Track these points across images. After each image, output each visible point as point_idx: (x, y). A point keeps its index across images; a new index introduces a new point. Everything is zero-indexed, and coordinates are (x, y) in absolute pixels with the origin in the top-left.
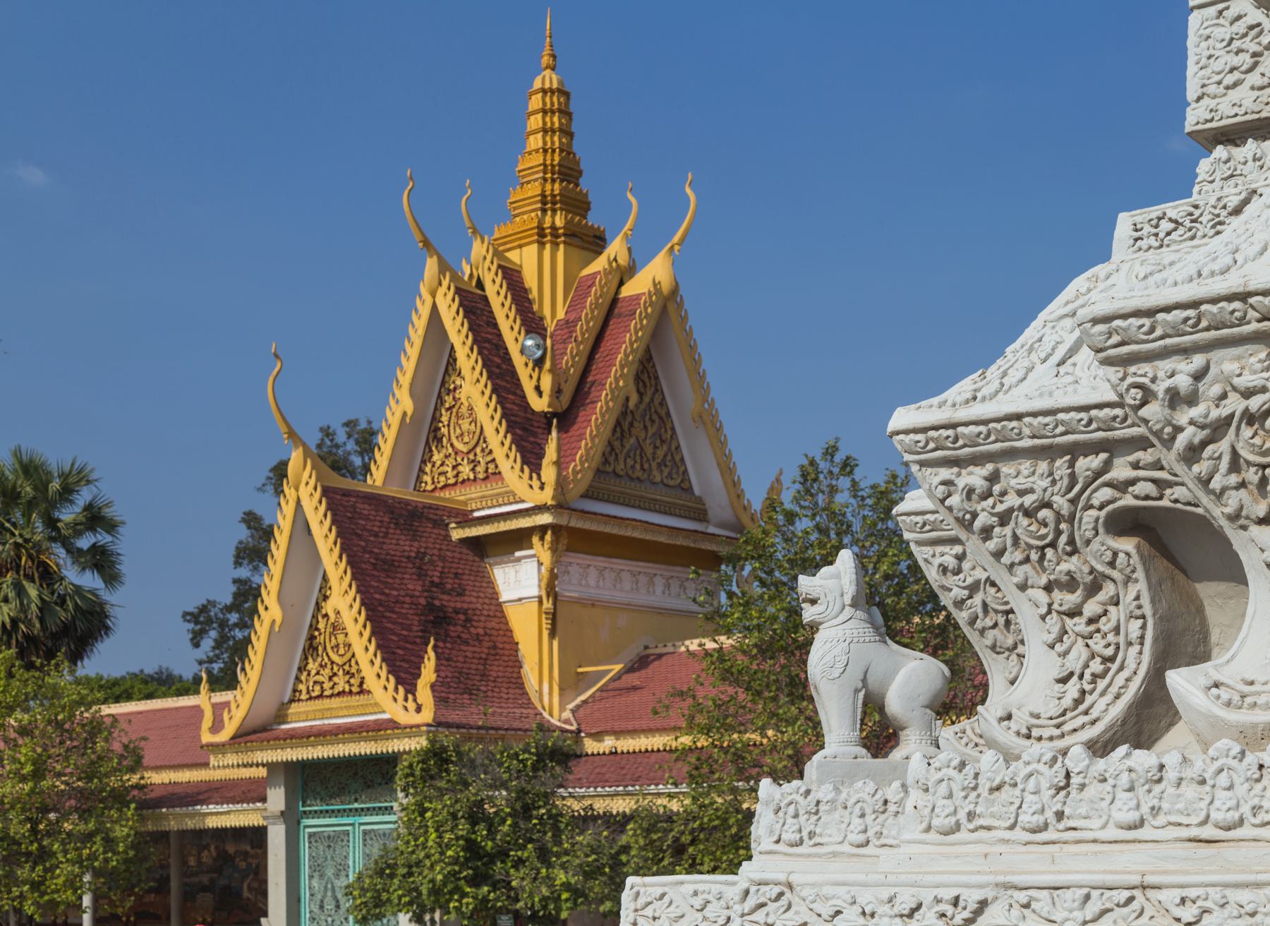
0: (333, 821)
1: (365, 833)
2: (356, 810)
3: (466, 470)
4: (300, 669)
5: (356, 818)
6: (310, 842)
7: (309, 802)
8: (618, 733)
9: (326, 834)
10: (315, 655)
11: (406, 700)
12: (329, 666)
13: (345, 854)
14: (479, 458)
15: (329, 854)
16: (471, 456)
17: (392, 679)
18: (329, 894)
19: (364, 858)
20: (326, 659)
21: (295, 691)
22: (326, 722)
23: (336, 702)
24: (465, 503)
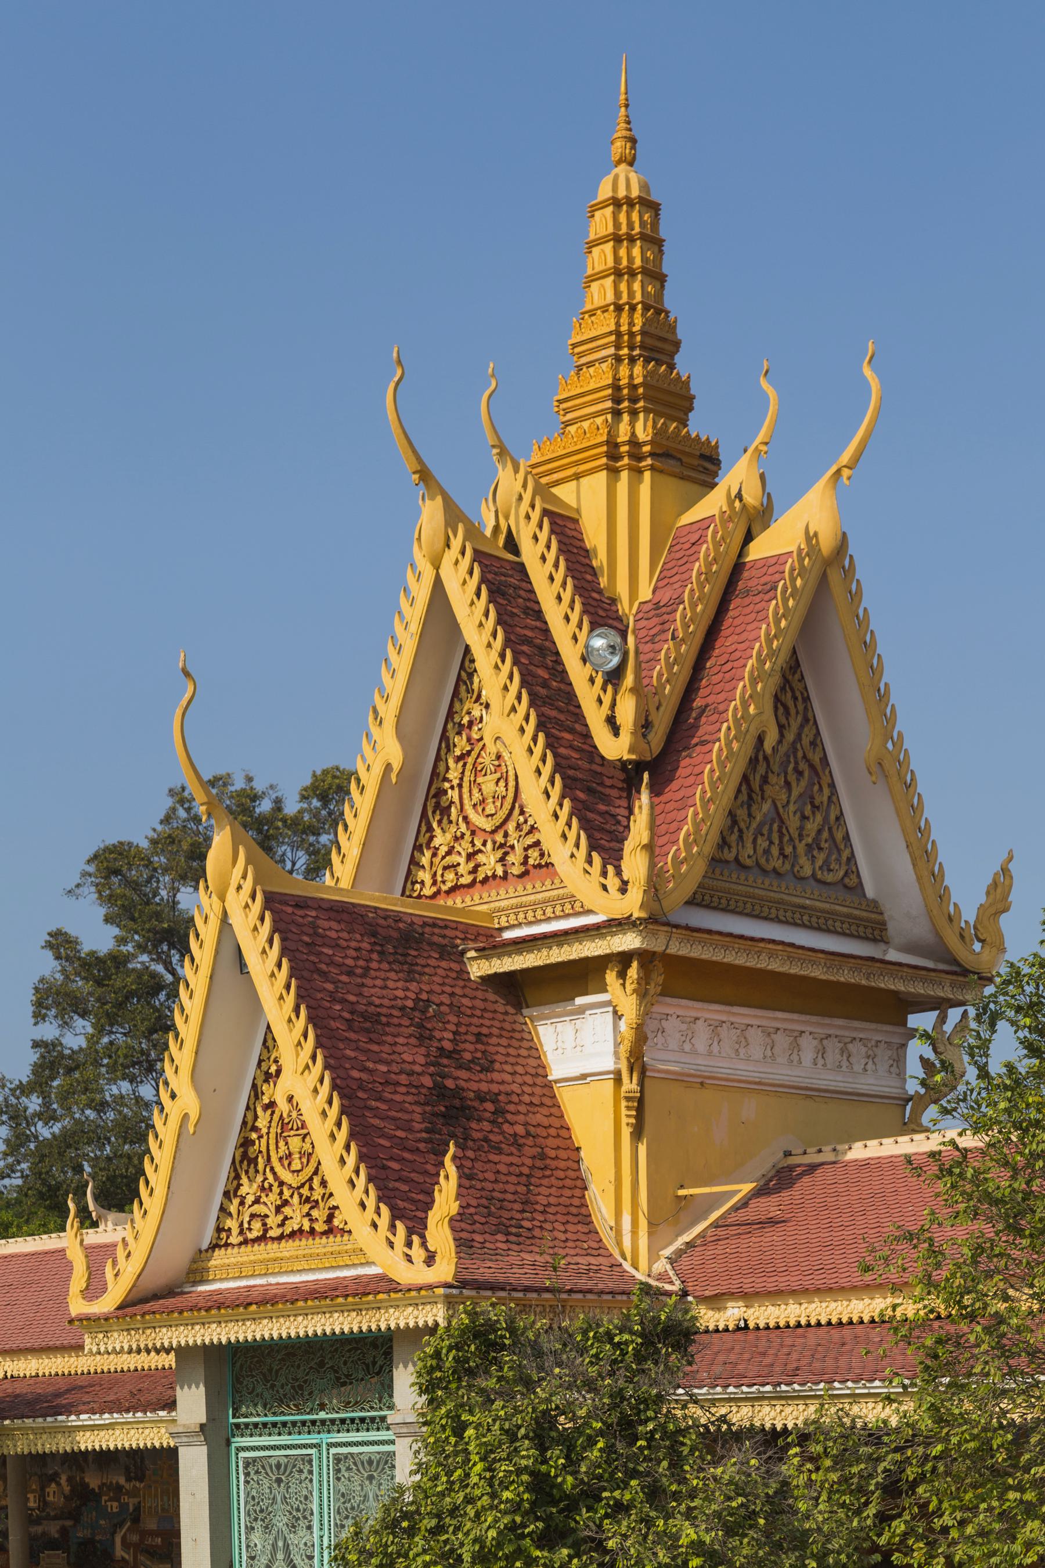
0: (285, 1439)
1: (338, 1459)
2: (323, 1422)
3: (489, 861)
4: (226, 1194)
5: (322, 1436)
6: (247, 1474)
7: (244, 1409)
8: (748, 1297)
9: (273, 1461)
10: (252, 1170)
11: (409, 1244)
12: (276, 1189)
13: (305, 1492)
14: (512, 840)
15: (279, 1492)
16: (499, 838)
17: (385, 1210)
18: (280, 1556)
19: (336, 1500)
20: (271, 1178)
21: (219, 1230)
22: (273, 1280)
23: (288, 1248)
24: (489, 916)
